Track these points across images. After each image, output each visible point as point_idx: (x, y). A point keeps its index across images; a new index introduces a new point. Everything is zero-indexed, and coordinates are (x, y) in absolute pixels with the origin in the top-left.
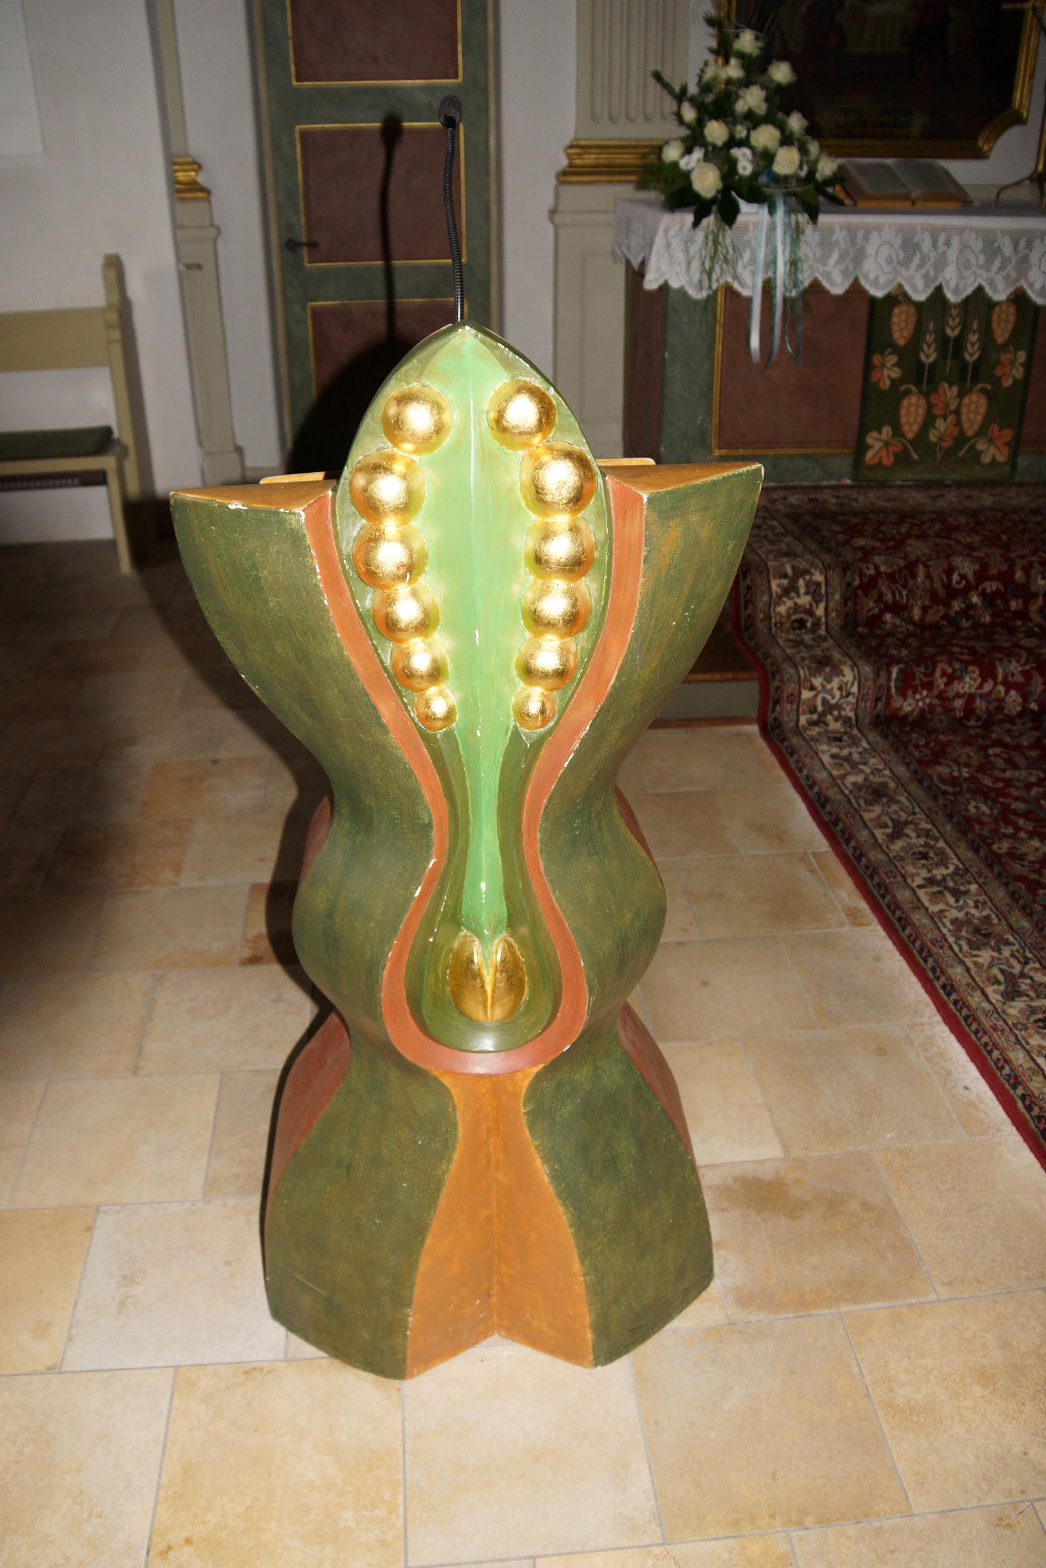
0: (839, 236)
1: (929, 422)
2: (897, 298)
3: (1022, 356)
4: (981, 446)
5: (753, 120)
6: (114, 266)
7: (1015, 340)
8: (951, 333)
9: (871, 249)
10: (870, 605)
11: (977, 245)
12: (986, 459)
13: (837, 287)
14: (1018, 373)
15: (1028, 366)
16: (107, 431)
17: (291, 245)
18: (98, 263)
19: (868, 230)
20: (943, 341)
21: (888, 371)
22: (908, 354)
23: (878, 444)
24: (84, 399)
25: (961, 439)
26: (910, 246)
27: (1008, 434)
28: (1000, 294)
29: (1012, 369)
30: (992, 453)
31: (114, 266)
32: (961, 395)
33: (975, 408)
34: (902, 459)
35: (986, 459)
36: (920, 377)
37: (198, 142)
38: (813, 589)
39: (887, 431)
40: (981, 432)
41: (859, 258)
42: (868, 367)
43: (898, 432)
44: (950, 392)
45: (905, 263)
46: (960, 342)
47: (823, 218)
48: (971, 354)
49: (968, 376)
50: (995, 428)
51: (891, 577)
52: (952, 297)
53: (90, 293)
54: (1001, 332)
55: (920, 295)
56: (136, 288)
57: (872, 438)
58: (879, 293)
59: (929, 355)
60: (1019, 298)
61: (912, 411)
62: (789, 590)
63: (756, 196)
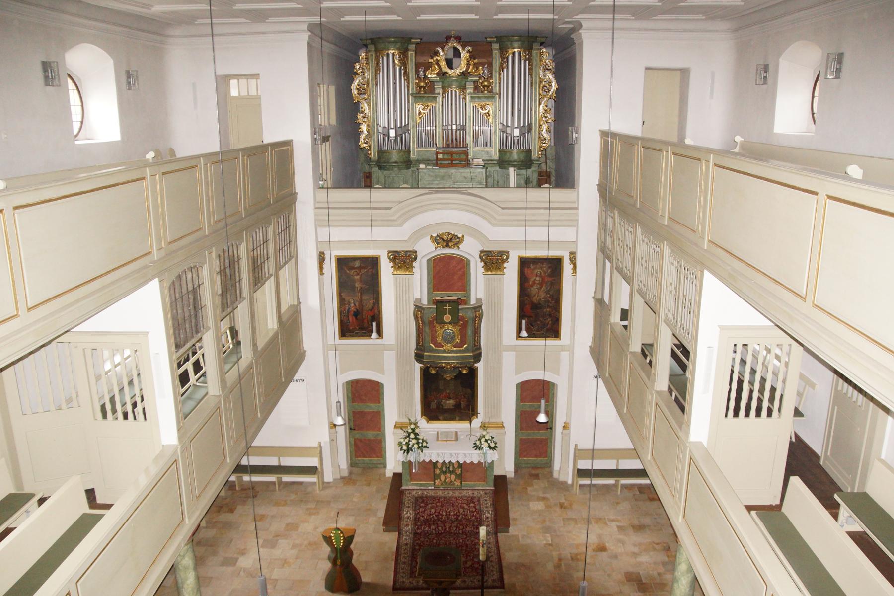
6: (320, 443)
13: (427, 461)
16: (316, 468)
17: (351, 429)
21: (438, 472)
22: (441, 469)
24: (313, 462)
26: (438, 454)
28: (454, 461)
29: (459, 471)
31: (320, 443)
33: (453, 477)
36: (444, 473)
48: (451, 469)
49: (452, 472)
54: (456, 466)
55: (441, 461)
59: (444, 469)
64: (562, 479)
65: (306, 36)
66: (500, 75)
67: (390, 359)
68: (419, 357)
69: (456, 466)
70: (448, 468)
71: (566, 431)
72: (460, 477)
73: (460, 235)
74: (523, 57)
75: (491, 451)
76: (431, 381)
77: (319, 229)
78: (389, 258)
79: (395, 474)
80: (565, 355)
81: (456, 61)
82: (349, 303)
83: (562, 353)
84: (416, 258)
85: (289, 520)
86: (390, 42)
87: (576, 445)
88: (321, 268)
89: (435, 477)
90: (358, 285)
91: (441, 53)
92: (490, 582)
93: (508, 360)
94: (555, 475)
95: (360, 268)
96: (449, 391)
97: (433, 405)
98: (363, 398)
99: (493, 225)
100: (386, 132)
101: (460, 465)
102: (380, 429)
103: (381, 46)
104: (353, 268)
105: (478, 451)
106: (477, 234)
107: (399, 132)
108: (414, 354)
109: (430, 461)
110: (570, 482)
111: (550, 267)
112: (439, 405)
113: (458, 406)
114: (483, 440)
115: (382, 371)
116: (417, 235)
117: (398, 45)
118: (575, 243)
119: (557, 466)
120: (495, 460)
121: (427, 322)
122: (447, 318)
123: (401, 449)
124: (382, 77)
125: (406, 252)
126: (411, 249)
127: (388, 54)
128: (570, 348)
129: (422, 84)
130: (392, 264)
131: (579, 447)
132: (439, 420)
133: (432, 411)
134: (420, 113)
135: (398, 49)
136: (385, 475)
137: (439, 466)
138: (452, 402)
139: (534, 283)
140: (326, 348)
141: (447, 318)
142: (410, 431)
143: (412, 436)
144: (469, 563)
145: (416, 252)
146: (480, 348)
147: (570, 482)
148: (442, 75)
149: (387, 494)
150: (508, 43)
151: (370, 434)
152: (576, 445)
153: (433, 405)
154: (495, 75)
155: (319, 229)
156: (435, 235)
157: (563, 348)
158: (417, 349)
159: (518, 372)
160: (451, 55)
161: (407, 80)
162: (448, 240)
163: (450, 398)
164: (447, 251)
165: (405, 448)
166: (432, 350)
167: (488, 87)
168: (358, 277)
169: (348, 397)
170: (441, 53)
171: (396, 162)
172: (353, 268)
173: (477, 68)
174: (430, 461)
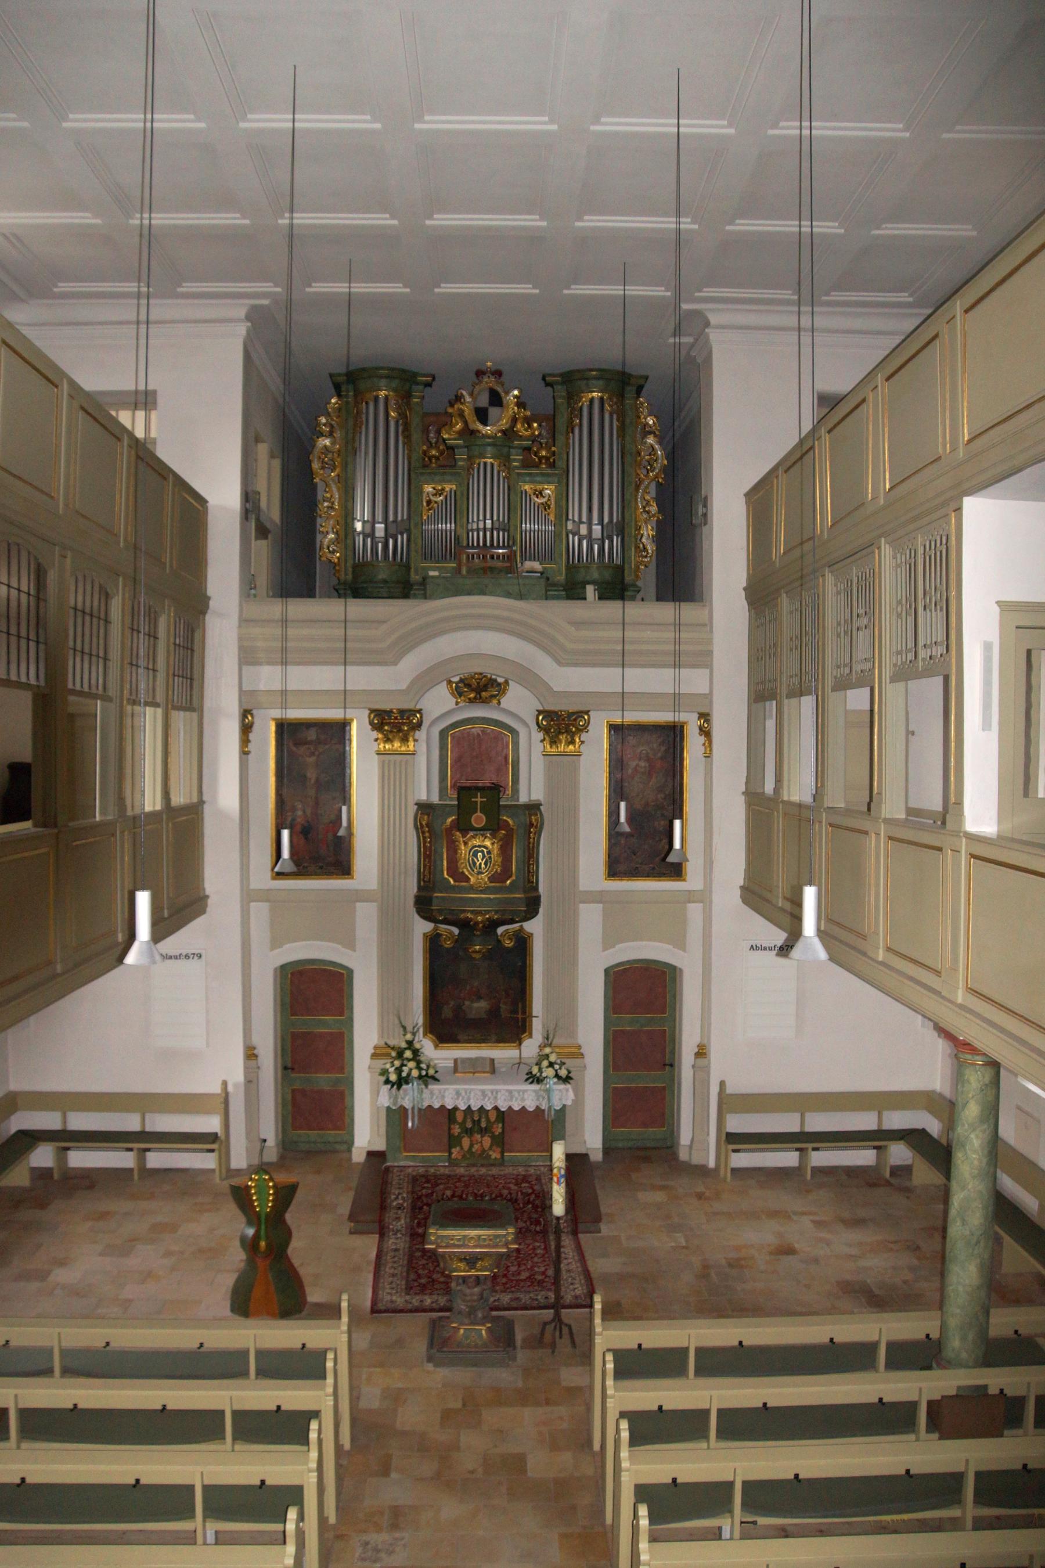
0: (436, 1092)
1: (471, 1146)
2: (456, 1109)
3: (500, 1125)
4: (491, 1153)
5: (409, 1060)
6: (225, 1084)
7: (497, 1120)
8: (476, 1118)
9: (447, 1094)
10: (419, 1204)
11: (480, 1094)
12: (493, 1157)
13: (436, 1106)
14: (500, 1130)
15: (503, 1128)
16: (216, 1134)
17: (285, 1068)
18: (220, 1082)
19: (445, 1090)
20: (474, 1121)
21: (456, 1130)
22: (463, 1124)
23: (455, 1151)
24: (211, 1124)
25: (484, 1151)
26: (458, 1093)
27: (499, 1149)
28: (489, 1107)
29: (498, 1129)
30: (495, 1155)
31: (225, 1084)
32: (482, 1137)
33: (487, 1141)
34: (464, 1156)
35: (493, 1157)
37: (256, 1040)
38: (403, 1198)
39: (458, 1148)
40: (490, 1148)
41: (443, 1097)
42: (450, 1129)
43: (462, 1148)
44: (478, 1137)
45: (458, 1099)
46: (479, 1121)
47: (430, 1087)
48: (483, 1125)
49: (483, 1131)
50: (494, 1148)
51: (427, 1196)
52: (474, 1109)
53: (217, 1089)
55: (463, 1107)
56: (230, 1089)
57: (453, 1150)
58: (450, 1107)
59: (469, 1125)
60: (496, 1108)
61: (466, 1142)
62: (397, 1198)
63: (407, 1083)
64: (696, 1160)
65: (242, 330)
66: (568, 439)
67: (366, 919)
68: (424, 906)
69: (493, 1117)
70: (477, 1121)
71: (701, 1062)
72: (500, 1142)
73: (500, 680)
74: (607, 407)
75: (562, 1086)
76: (442, 968)
77: (244, 668)
78: (371, 723)
79: (370, 1154)
80: (694, 910)
81: (493, 412)
82: (294, 809)
83: (691, 906)
84: (419, 725)
85: (160, 1218)
86: (382, 377)
87: (722, 1084)
88: (245, 741)
89: (453, 1141)
90: (312, 774)
91: (468, 399)
92: (568, 1298)
93: (590, 920)
94: (683, 1155)
95: (319, 742)
96: (477, 980)
97: (447, 1012)
98: (311, 997)
99: (560, 663)
100: (368, 530)
101: (502, 1115)
102: (341, 1070)
103: (362, 385)
104: (306, 743)
105: (535, 1087)
106: (531, 679)
107: (392, 531)
108: (411, 901)
109: (443, 1107)
110: (712, 1164)
111: (662, 743)
112: (458, 1010)
113: (494, 1012)
114: (545, 1063)
115: (350, 944)
116: (423, 682)
117: (395, 383)
118: (709, 697)
119: (685, 1137)
120: (569, 1103)
121: (436, 829)
122: (478, 819)
123: (387, 1082)
124: (365, 441)
125: (402, 712)
126: (411, 706)
127: (376, 398)
128: (704, 897)
129: (434, 452)
130: (375, 734)
131: (729, 1090)
132: (457, 1041)
133: (444, 1026)
134: (429, 502)
135: (395, 390)
136: (350, 1159)
137: (459, 1117)
138: (482, 1005)
139: (635, 770)
140: (249, 896)
141: (478, 819)
142: (404, 1045)
143: (408, 1054)
144: (524, 1275)
145: (419, 711)
146: (536, 889)
147: (712, 1164)
148: (469, 433)
149: (354, 1184)
150: (583, 383)
151: (323, 1080)
152: (722, 1084)
153: (447, 1012)
154: (560, 439)
155: (244, 668)
156: (456, 679)
157: (690, 897)
158: (419, 888)
159: (609, 942)
160: (484, 401)
161: (408, 437)
162: (480, 688)
163: (479, 998)
164: (479, 712)
165: (393, 1077)
166: (449, 888)
167: (547, 458)
168: (312, 759)
169: (283, 1004)
170: (468, 399)
171: (385, 581)
172: (306, 743)
173: (530, 426)
174: (443, 1107)
